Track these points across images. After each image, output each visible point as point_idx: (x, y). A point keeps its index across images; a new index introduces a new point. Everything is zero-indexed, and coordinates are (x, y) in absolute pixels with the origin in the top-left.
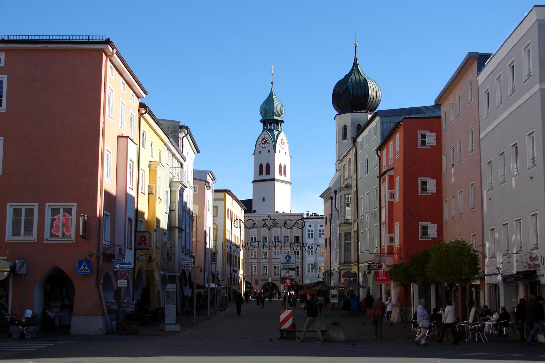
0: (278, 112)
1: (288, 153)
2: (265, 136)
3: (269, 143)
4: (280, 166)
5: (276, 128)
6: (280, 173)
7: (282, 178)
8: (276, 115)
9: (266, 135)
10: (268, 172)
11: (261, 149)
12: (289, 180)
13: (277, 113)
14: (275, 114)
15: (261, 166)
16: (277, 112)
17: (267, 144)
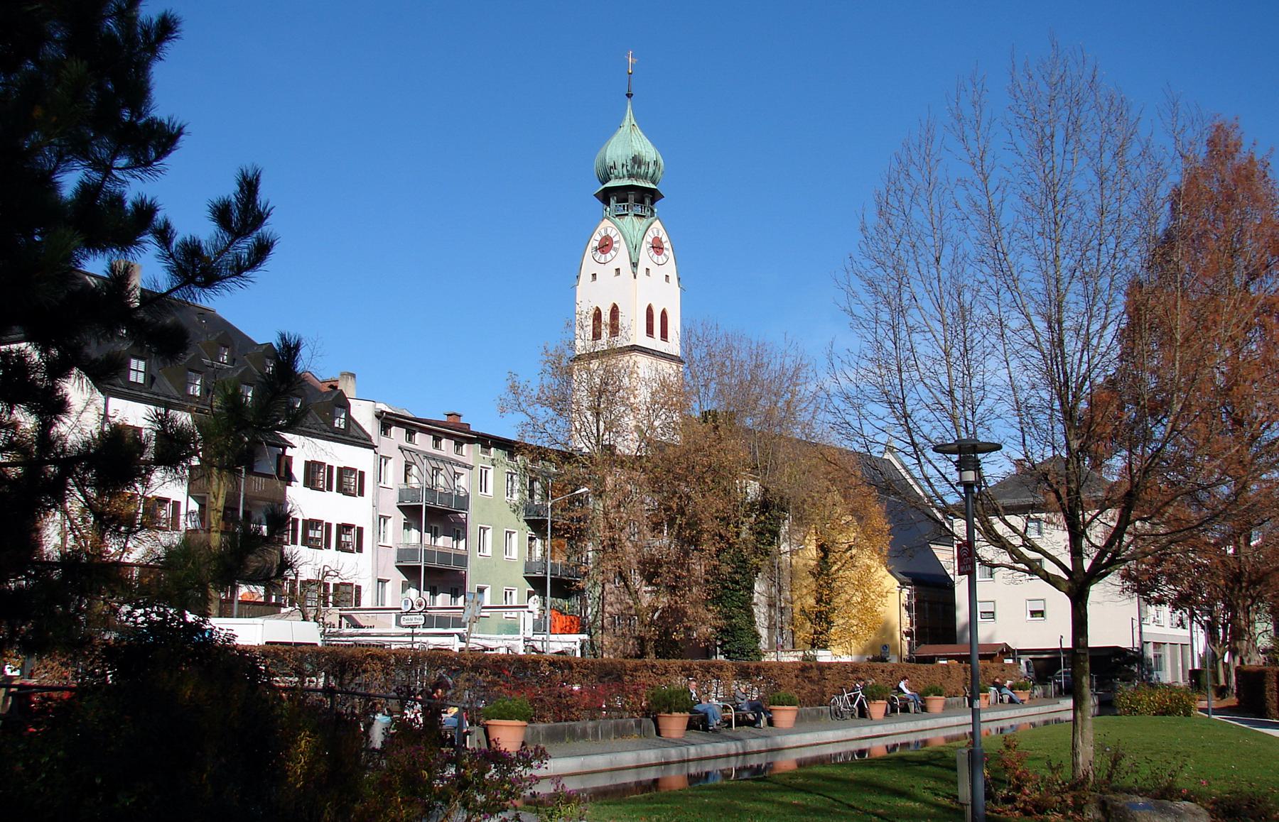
1: (674, 278)
3: (616, 250)
6: (650, 331)
7: (656, 343)
9: (609, 230)
10: (615, 330)
11: (597, 269)
15: (597, 316)
17: (612, 251)
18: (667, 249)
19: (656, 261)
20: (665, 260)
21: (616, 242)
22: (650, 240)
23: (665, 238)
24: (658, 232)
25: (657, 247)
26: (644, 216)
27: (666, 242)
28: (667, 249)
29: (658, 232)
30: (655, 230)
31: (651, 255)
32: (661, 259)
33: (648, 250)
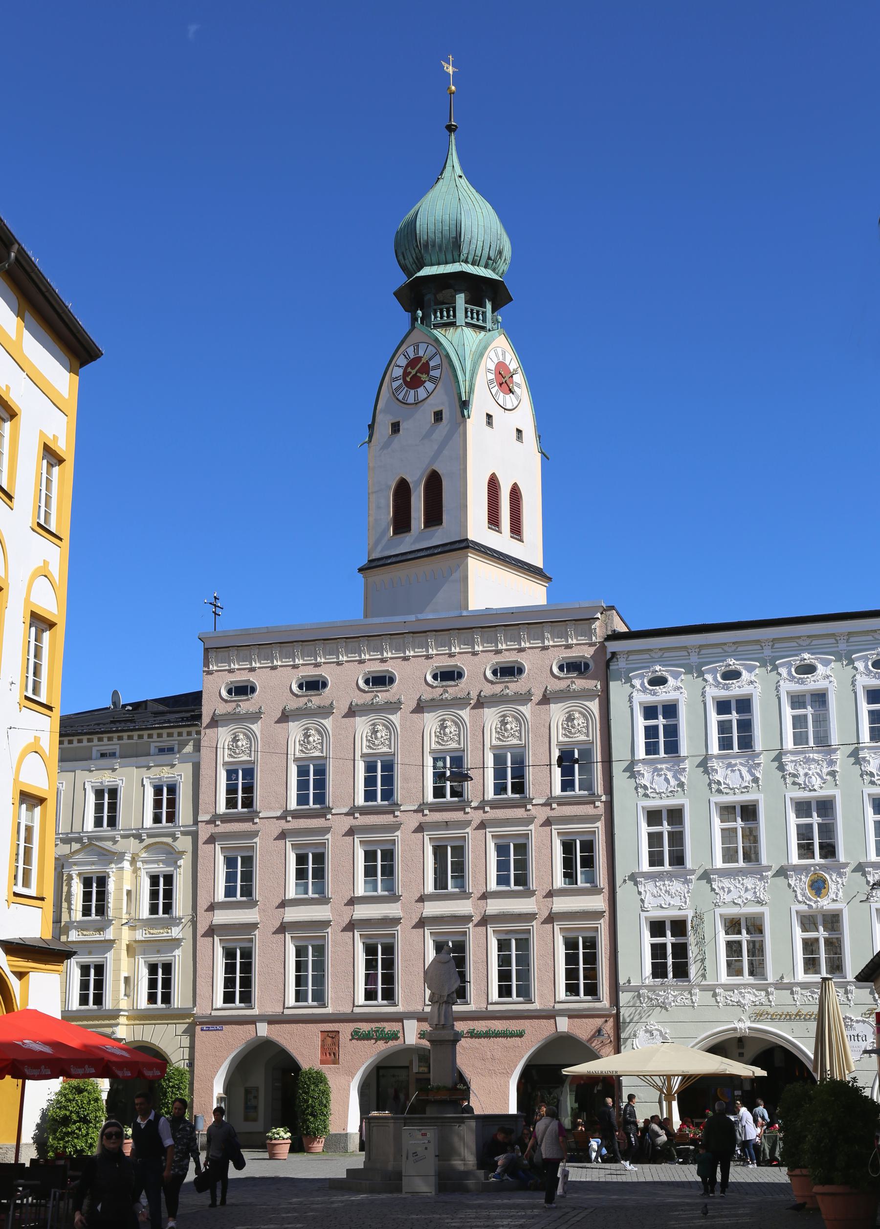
0: (480, 244)
1: (530, 434)
2: (416, 350)
4: (493, 484)
5: (478, 320)
6: (494, 520)
8: (470, 259)
10: (434, 516)
12: (539, 562)
13: (473, 246)
14: (465, 251)
15: (403, 491)
16: (474, 241)
18: (519, 386)
21: (435, 368)
22: (492, 366)
24: (504, 354)
25: (504, 381)
26: (482, 328)
27: (516, 371)
28: (519, 386)
29: (504, 354)
30: (499, 351)
31: (494, 391)
32: (510, 401)
33: (490, 382)
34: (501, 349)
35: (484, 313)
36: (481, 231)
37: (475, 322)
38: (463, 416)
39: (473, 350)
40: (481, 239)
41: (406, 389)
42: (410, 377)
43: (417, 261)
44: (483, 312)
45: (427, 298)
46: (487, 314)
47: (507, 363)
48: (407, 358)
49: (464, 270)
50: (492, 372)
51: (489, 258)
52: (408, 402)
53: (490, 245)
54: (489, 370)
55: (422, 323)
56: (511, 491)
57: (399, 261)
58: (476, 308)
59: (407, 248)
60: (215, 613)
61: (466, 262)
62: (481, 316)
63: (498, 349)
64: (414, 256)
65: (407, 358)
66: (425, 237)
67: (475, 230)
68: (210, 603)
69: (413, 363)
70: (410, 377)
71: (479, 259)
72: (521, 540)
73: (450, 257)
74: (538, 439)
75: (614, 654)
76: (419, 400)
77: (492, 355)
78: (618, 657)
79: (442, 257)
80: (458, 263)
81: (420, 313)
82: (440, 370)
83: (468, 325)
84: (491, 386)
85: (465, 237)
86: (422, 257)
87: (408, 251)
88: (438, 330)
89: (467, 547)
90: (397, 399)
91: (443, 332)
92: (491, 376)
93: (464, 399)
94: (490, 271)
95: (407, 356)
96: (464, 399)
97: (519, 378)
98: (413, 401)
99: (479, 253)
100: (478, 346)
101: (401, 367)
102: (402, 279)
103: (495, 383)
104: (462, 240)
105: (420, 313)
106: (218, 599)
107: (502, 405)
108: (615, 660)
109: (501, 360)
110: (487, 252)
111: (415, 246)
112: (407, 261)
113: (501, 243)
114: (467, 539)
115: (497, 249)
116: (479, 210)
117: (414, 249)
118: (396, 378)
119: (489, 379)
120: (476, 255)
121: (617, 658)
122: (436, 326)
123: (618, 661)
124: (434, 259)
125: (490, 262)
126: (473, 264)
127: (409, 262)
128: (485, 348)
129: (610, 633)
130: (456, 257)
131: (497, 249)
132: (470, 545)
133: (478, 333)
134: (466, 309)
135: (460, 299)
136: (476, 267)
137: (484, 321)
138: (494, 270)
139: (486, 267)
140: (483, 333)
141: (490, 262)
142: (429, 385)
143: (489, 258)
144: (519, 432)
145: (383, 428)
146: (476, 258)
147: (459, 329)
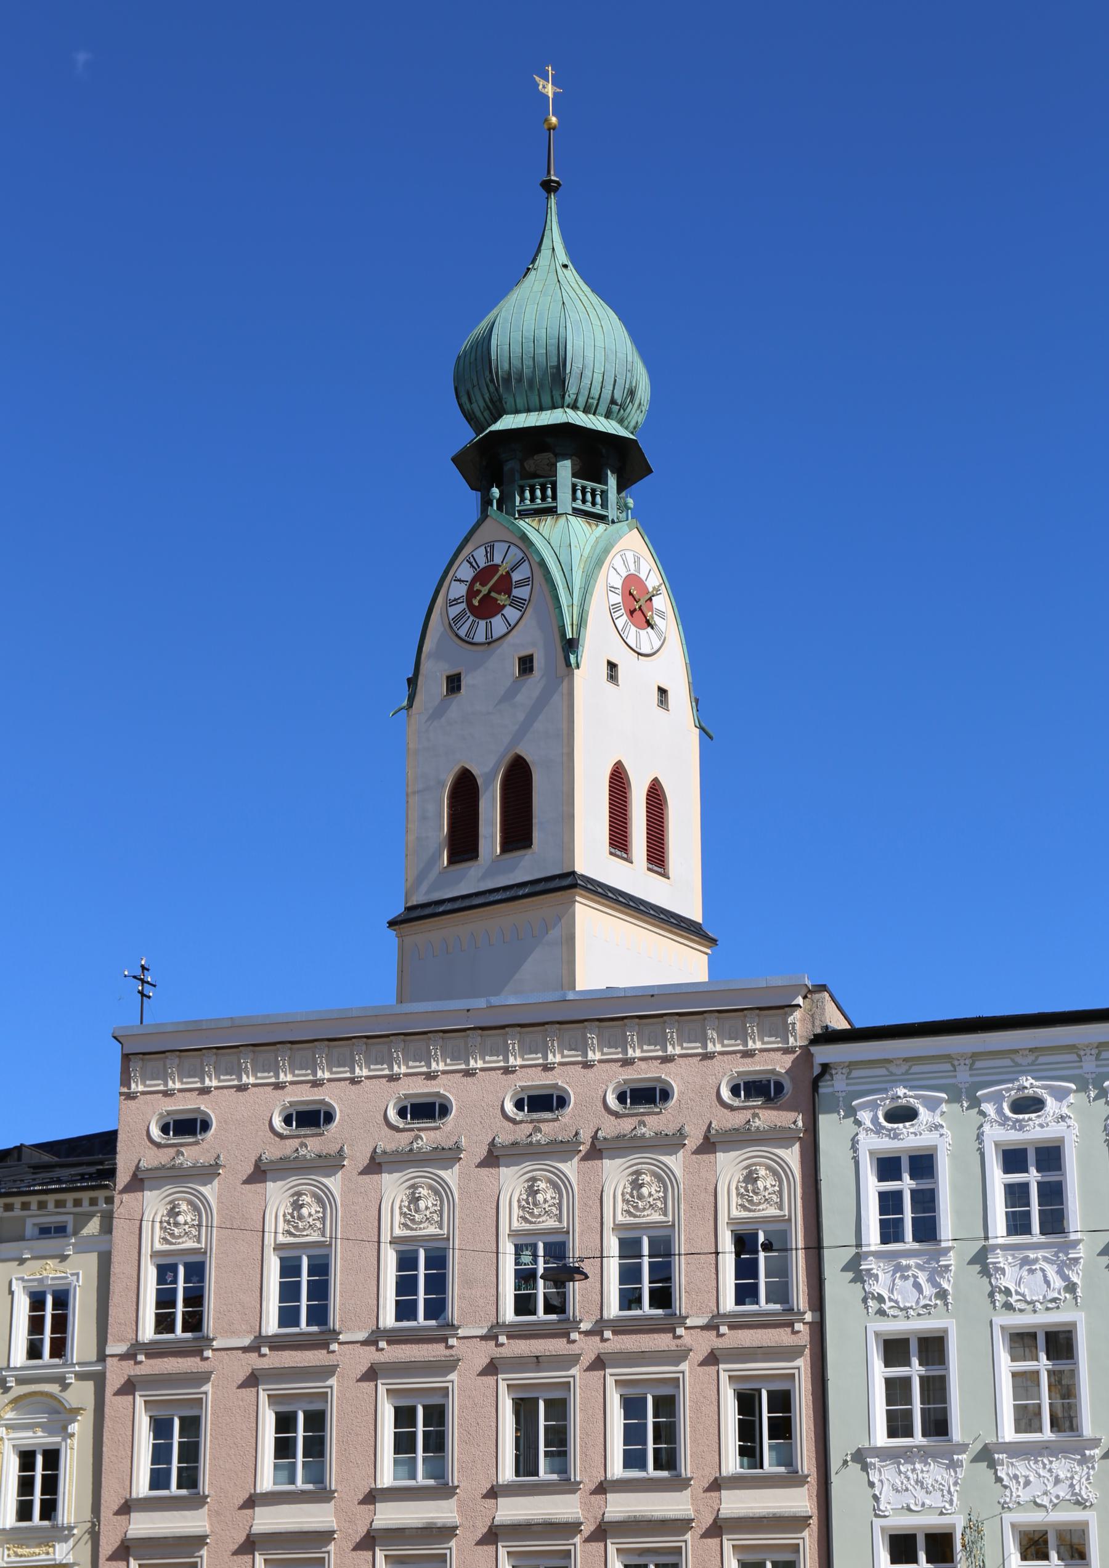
0: (598, 378)
4: (619, 781)
5: (594, 504)
6: (619, 841)
8: (581, 403)
12: (695, 914)
13: (586, 382)
14: (572, 390)
16: (588, 373)
19: (632, 641)
20: (657, 644)
21: (521, 584)
22: (618, 583)
23: (653, 578)
24: (637, 561)
26: (602, 518)
28: (662, 614)
29: (637, 561)
30: (630, 556)
31: (620, 623)
32: (646, 640)
34: (632, 553)
35: (604, 494)
36: (600, 356)
37: (588, 507)
38: (568, 664)
39: (586, 554)
40: (599, 370)
41: (472, 618)
42: (478, 598)
43: (491, 406)
44: (602, 492)
45: (507, 467)
46: (609, 495)
47: (643, 576)
48: (473, 567)
49: (571, 421)
50: (617, 591)
51: (613, 401)
52: (475, 640)
53: (615, 381)
54: (612, 589)
55: (500, 508)
56: (649, 791)
57: (460, 405)
58: (590, 485)
59: (475, 383)
60: (142, 993)
61: (574, 407)
62: (598, 499)
63: (626, 552)
64: (487, 396)
65: (473, 567)
66: (506, 366)
67: (589, 354)
68: (135, 977)
69: (484, 575)
70: (478, 598)
71: (595, 402)
72: (665, 875)
73: (546, 400)
74: (694, 704)
75: (825, 1068)
76: (494, 638)
77: (618, 562)
78: (834, 1072)
79: (534, 400)
80: (560, 410)
81: (496, 492)
82: (530, 587)
83: (577, 512)
84: (615, 615)
85: (573, 366)
86: (500, 399)
87: (476, 389)
88: (527, 520)
89: (574, 886)
90: (457, 635)
91: (535, 524)
92: (617, 599)
93: (569, 636)
94: (614, 423)
95: (474, 564)
96: (569, 636)
97: (662, 602)
98: (483, 640)
99: (595, 393)
100: (594, 547)
101: (463, 581)
102: (465, 436)
103: (623, 611)
104: (568, 371)
105: (496, 492)
106: (148, 970)
107: (634, 647)
108: (827, 1077)
109: (632, 572)
110: (610, 392)
111: (488, 380)
112: (474, 405)
113: (632, 376)
114: (573, 873)
115: (627, 386)
116: (596, 322)
117: (487, 386)
118: (455, 600)
119: (611, 603)
120: (591, 396)
121: (831, 1075)
122: (523, 514)
123: (833, 1080)
124: (520, 405)
125: (615, 408)
126: (586, 411)
127: (478, 407)
128: (606, 551)
129: (819, 1031)
130: (558, 398)
131: (627, 386)
132: (579, 882)
133: (594, 527)
134: (574, 486)
135: (564, 469)
136: (591, 416)
137: (604, 505)
138: (621, 422)
139: (608, 415)
140: (602, 526)
141: (615, 408)
142: (511, 613)
143: (613, 401)
144: (662, 692)
145: (433, 685)
146: (590, 401)
147: (563, 520)
